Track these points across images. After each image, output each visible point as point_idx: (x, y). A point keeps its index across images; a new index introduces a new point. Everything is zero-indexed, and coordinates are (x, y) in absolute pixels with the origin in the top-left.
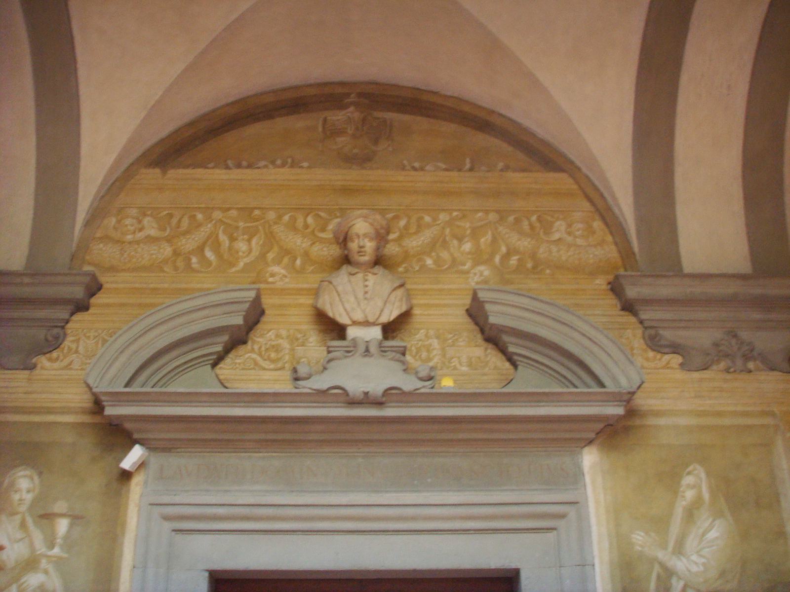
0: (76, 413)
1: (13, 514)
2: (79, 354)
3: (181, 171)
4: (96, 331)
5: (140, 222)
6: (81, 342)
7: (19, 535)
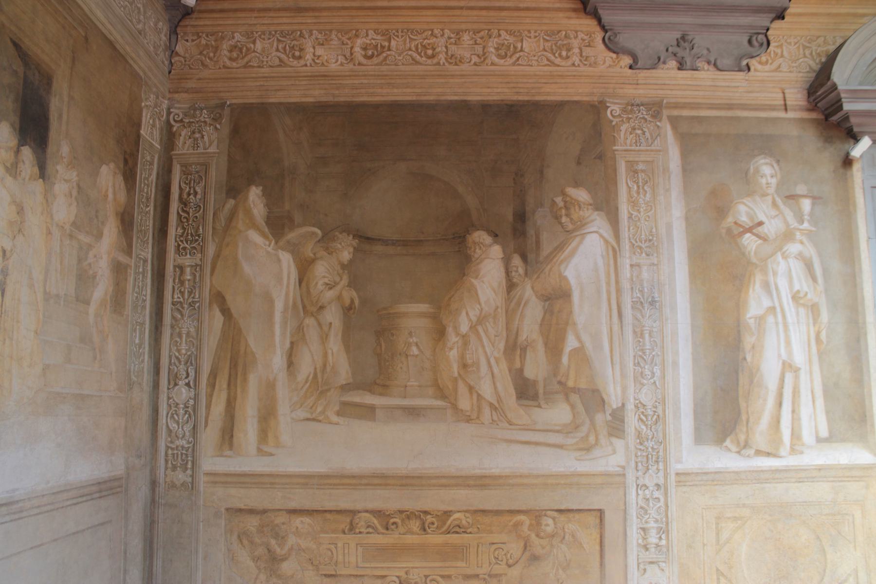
0: (795, 110)
1: (765, 195)
4: (794, 38)
6: (784, 48)
7: (773, 212)
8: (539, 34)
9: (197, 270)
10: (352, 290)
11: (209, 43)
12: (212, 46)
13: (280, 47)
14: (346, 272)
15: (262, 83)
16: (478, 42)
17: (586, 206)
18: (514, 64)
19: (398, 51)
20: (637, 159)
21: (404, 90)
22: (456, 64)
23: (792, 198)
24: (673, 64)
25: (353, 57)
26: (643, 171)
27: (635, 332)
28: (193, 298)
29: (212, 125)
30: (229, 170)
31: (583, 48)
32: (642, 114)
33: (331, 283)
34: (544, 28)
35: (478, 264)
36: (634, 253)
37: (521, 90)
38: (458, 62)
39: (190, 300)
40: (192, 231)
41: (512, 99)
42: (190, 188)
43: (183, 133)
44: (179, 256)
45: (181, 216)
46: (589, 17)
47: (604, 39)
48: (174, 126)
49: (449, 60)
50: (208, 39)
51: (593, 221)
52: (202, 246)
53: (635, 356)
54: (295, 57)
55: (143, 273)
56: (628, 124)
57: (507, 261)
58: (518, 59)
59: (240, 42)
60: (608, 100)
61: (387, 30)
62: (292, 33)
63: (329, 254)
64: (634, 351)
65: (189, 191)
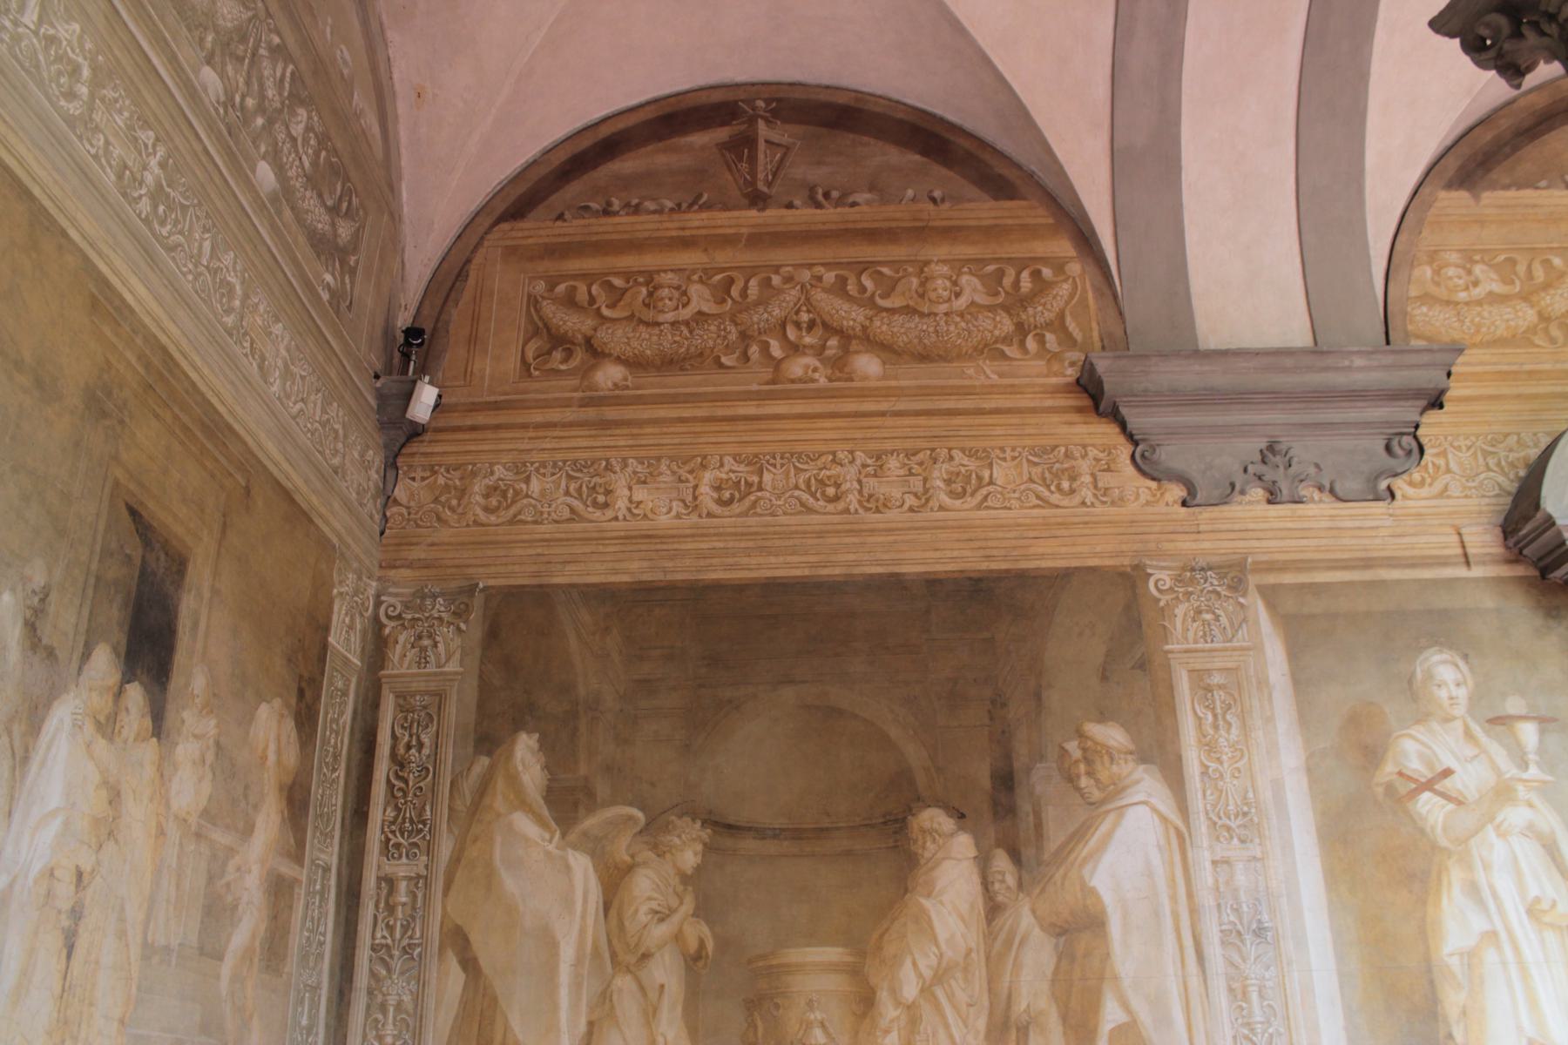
0: (1484, 563)
1: (1448, 719)
2: (1455, 473)
3: (1501, 193)
5: (1469, 272)
6: (1450, 456)
7: (1469, 751)
8: (1020, 453)
9: (420, 885)
10: (703, 923)
11: (450, 482)
12: (455, 488)
13: (573, 487)
14: (690, 888)
15: (539, 550)
16: (913, 471)
17: (1122, 756)
18: (979, 507)
19: (776, 491)
20: (1208, 666)
21: (789, 559)
22: (878, 511)
23: (1500, 722)
24: (1258, 493)
25: (697, 503)
26: (1220, 687)
27: (1231, 990)
28: (411, 938)
29: (453, 624)
30: (481, 706)
31: (1098, 473)
32: (1212, 584)
33: (663, 910)
34: (1028, 442)
35: (932, 869)
36: (1218, 839)
37: (995, 552)
38: (881, 509)
39: (405, 942)
40: (413, 814)
41: (978, 568)
42: (411, 736)
43: (402, 639)
44: (388, 859)
45: (394, 786)
46: (1104, 420)
47: (1133, 457)
48: (385, 626)
49: (865, 504)
50: (449, 476)
51: (1138, 782)
52: (429, 841)
53: (1235, 1037)
54: (597, 503)
55: (323, 893)
56: (1187, 604)
57: (983, 862)
58: (986, 498)
59: (502, 480)
60: (1148, 562)
61: (756, 456)
62: (593, 464)
63: (658, 856)
64: (1233, 1028)
65: (409, 742)
